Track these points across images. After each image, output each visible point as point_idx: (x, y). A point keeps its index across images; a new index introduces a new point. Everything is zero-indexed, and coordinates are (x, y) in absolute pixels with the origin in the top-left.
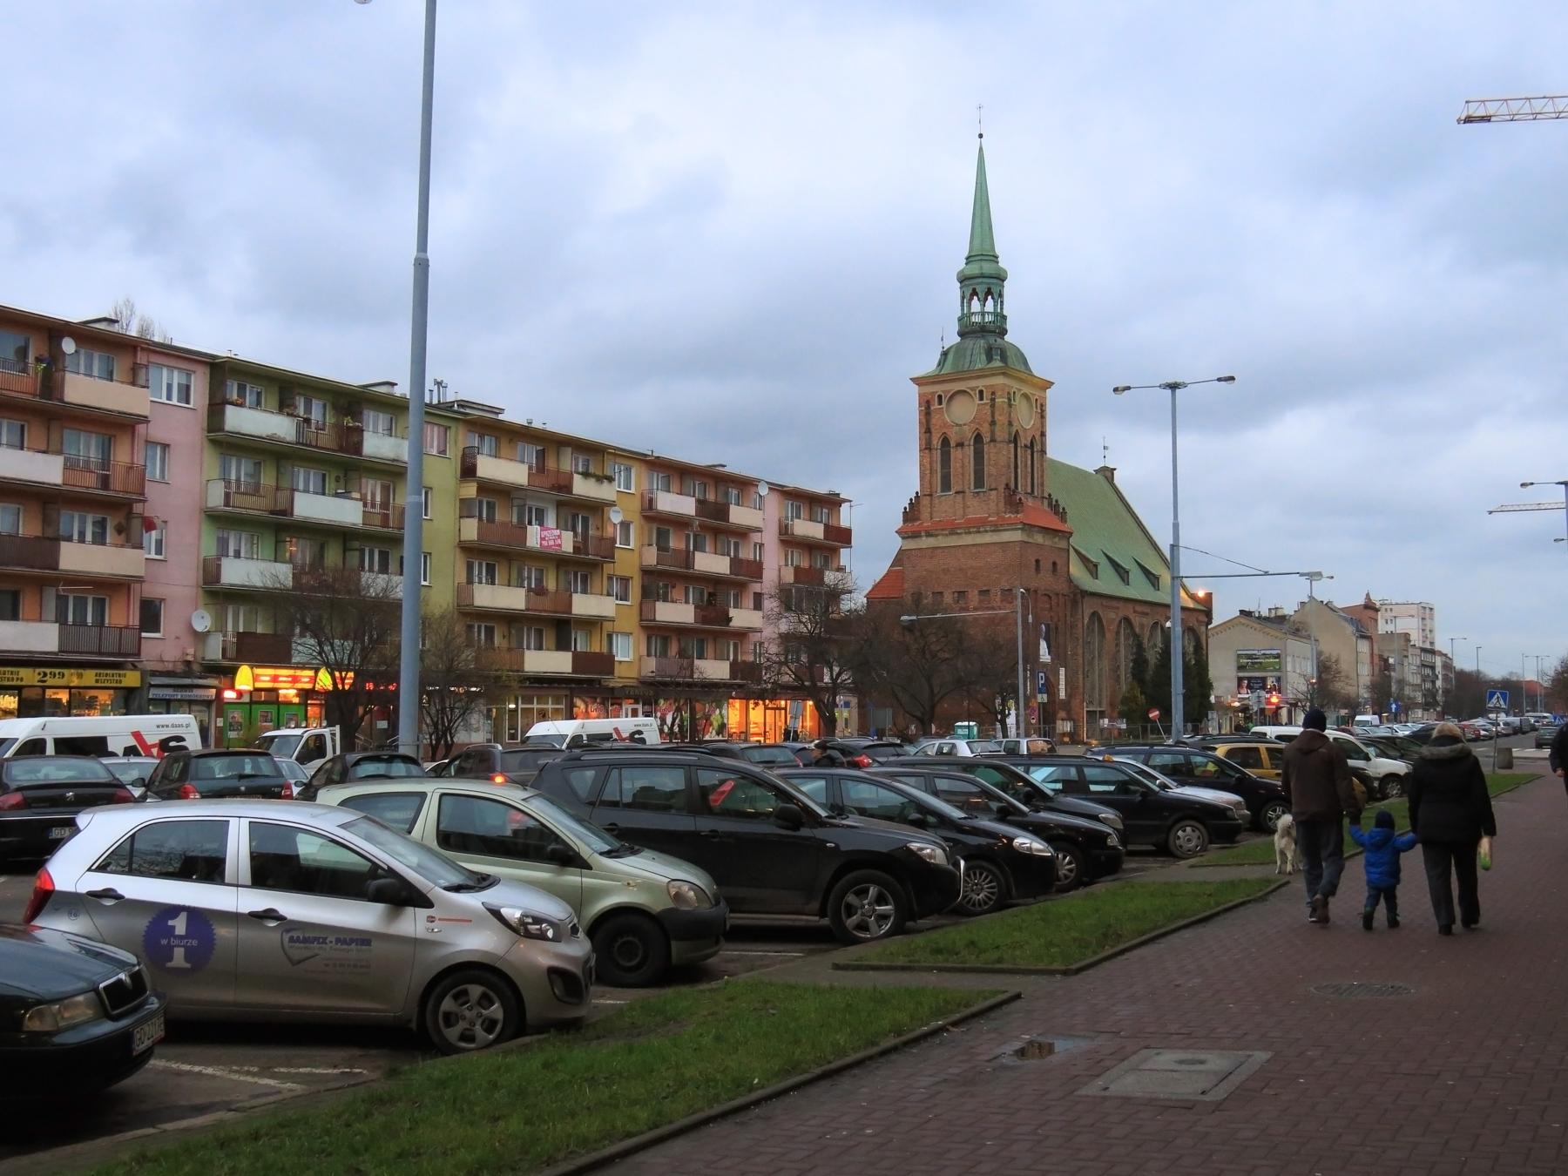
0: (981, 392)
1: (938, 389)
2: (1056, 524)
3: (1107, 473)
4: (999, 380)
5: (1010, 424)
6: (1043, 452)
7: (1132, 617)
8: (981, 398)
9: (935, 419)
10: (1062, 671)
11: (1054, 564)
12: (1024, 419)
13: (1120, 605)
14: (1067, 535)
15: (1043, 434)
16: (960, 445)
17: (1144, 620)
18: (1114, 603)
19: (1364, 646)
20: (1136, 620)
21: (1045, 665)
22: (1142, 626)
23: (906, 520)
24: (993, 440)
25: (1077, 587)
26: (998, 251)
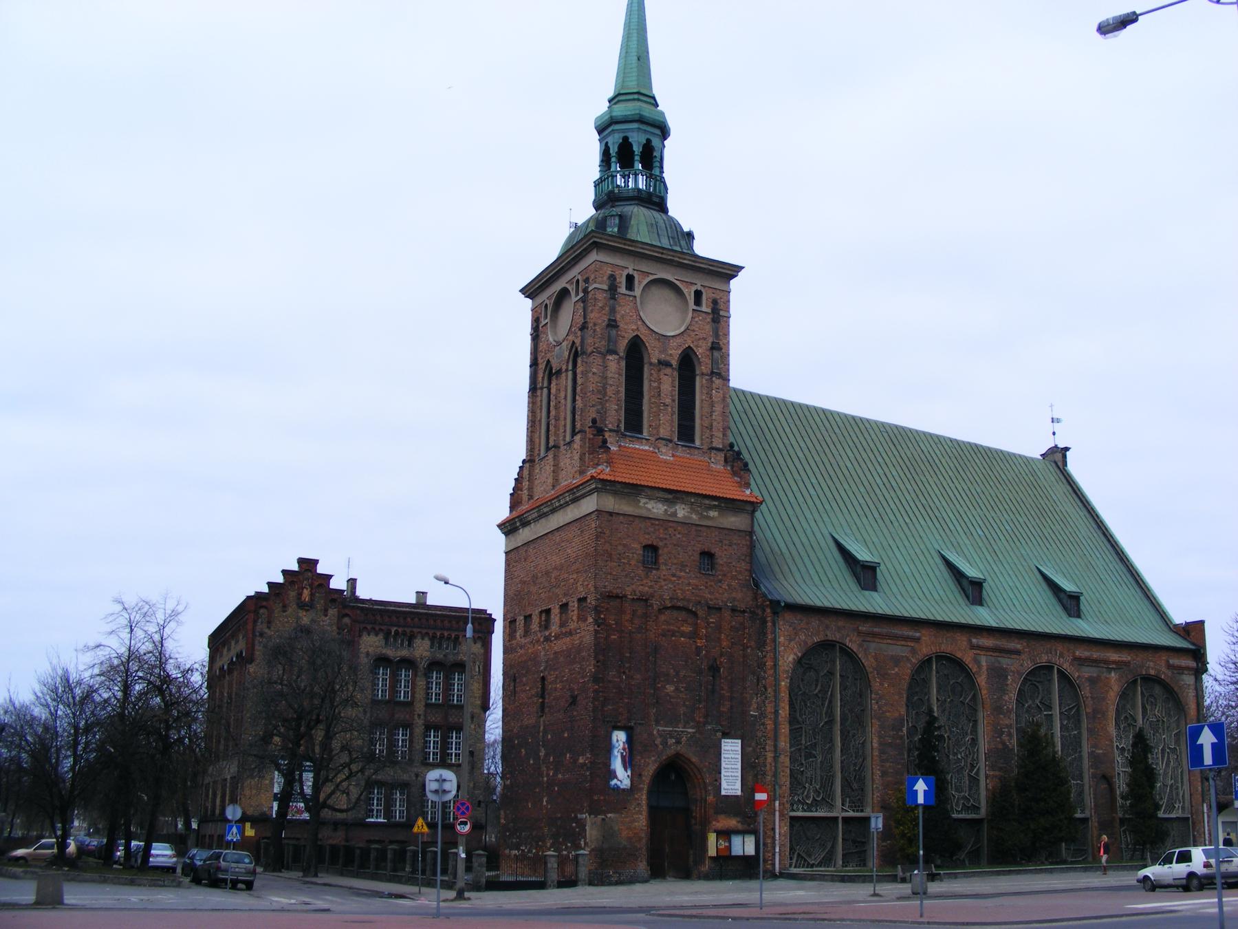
0: (578, 281)
2: (729, 490)
3: (1057, 456)
4: (594, 256)
5: (612, 324)
6: (720, 372)
7: (967, 658)
8: (577, 294)
9: (542, 346)
10: (731, 750)
11: (708, 555)
12: (663, 319)
13: (926, 635)
16: (559, 372)
17: (1005, 662)
23: (512, 508)
24: (583, 353)
25: (764, 595)
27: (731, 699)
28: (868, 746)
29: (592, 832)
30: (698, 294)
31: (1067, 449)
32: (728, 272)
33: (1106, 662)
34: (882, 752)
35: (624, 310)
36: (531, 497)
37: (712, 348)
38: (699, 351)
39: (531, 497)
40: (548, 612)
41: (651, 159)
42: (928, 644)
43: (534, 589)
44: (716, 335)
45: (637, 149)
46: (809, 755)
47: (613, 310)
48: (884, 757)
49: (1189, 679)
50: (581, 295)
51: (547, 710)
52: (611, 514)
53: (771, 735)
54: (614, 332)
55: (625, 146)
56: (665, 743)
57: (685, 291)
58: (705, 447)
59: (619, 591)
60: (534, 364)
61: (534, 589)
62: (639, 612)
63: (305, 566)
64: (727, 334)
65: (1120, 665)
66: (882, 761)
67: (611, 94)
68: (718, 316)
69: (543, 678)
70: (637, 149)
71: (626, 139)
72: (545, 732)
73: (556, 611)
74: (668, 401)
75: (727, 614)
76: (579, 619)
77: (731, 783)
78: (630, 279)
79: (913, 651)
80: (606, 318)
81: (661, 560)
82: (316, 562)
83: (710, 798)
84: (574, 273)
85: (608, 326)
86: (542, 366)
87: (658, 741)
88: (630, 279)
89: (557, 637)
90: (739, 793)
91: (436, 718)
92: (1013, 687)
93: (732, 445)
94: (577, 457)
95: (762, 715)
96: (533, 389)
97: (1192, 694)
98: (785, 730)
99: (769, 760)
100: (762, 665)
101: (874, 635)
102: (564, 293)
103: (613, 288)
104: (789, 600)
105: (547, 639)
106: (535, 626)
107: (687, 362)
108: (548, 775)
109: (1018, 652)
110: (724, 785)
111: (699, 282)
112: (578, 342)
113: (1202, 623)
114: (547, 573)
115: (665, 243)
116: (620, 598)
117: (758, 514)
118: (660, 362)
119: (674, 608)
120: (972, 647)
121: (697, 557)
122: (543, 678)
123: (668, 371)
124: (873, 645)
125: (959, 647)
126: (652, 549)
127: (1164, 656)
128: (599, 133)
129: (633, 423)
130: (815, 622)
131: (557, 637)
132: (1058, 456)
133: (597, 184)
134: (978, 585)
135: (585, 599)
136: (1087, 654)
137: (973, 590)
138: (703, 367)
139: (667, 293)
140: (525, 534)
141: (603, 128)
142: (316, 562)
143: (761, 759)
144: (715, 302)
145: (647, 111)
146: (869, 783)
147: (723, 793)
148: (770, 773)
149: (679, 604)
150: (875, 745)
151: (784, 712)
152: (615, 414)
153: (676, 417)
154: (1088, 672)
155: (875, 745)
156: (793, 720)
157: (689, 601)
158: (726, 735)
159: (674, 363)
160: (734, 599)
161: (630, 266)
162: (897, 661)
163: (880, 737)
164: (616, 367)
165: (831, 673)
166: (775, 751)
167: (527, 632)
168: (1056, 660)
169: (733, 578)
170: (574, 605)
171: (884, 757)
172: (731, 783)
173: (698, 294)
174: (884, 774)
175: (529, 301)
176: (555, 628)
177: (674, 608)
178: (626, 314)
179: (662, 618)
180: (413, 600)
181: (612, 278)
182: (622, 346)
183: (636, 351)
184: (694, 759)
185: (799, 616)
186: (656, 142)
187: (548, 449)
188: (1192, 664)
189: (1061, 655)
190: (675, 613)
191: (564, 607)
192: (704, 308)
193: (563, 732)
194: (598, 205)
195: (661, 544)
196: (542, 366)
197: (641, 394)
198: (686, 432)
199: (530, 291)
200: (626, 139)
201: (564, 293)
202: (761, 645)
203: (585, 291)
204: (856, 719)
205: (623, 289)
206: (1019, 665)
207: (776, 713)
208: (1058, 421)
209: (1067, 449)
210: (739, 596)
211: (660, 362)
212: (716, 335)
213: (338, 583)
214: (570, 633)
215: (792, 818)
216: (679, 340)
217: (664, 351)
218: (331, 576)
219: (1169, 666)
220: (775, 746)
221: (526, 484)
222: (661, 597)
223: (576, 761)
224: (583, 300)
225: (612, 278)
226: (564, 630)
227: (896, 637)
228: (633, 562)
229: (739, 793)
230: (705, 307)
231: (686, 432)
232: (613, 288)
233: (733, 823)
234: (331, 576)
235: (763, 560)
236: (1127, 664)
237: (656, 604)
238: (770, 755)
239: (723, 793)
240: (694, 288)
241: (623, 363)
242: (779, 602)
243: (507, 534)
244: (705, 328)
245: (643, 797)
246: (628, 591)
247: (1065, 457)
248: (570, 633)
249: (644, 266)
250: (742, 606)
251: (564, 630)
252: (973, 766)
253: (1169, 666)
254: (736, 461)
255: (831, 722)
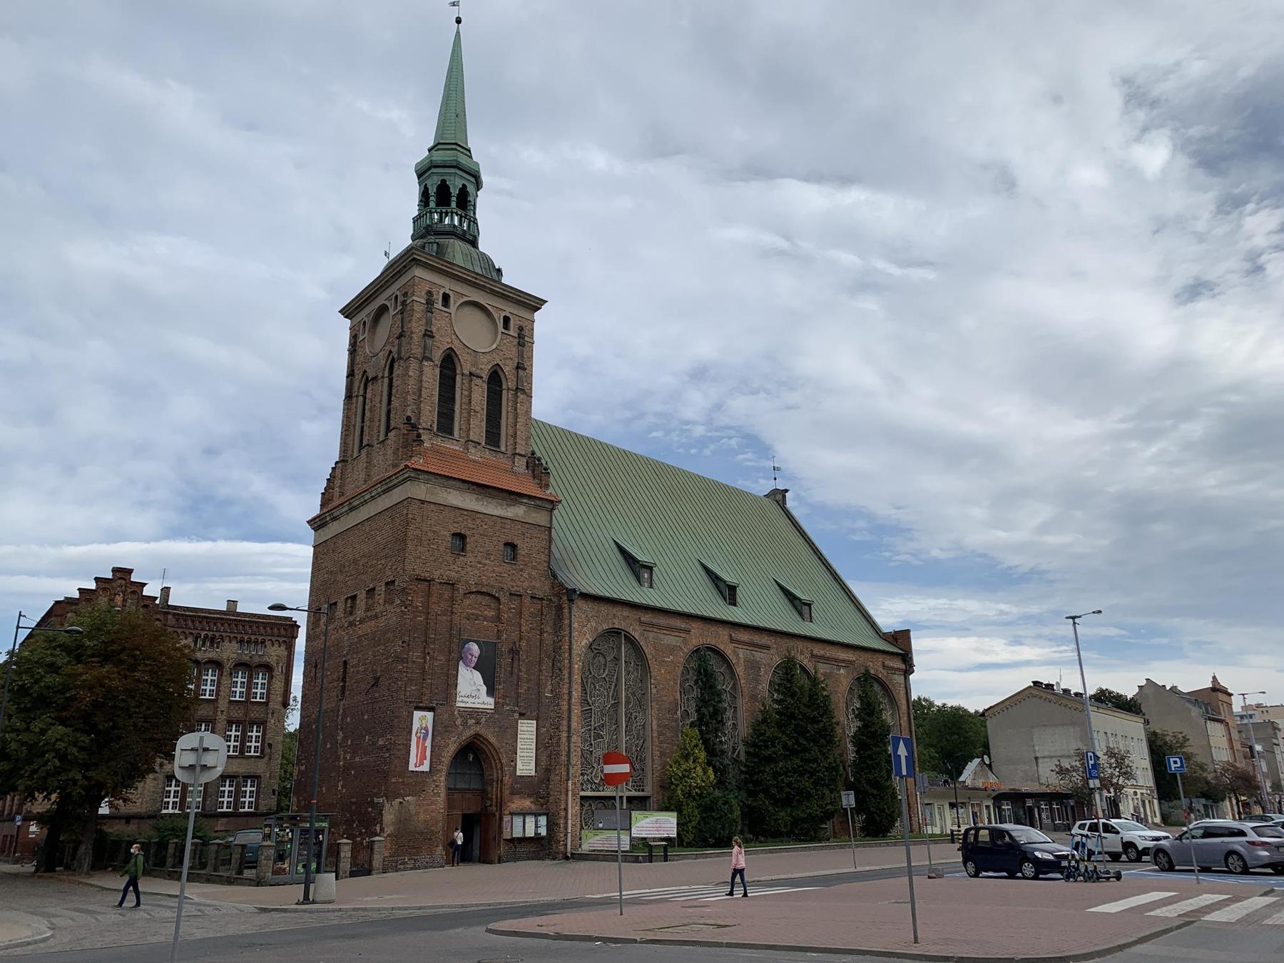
1: (362, 315)
2: (531, 488)
3: (778, 497)
5: (428, 334)
6: (523, 390)
7: (728, 650)
9: (359, 359)
10: (527, 731)
11: (511, 546)
12: (473, 336)
13: (695, 627)
14: (551, 505)
15: (523, 368)
16: (375, 379)
17: (758, 655)
18: (678, 623)
19: (1216, 732)
20: (739, 656)
21: (474, 713)
22: (753, 666)
23: (322, 506)
25: (561, 585)
26: (471, 144)
27: (528, 681)
28: (648, 727)
29: (389, 816)
30: (506, 320)
31: (786, 491)
32: (534, 304)
33: (836, 660)
34: (660, 734)
35: (438, 325)
36: (342, 494)
37: (518, 368)
38: (506, 369)
39: (342, 494)
40: (354, 598)
41: (465, 202)
42: (698, 636)
43: (340, 578)
44: (521, 355)
45: (454, 191)
46: (599, 736)
47: (429, 322)
48: (662, 738)
49: (900, 679)
50: (399, 308)
51: (347, 693)
52: (423, 502)
53: (565, 716)
54: (429, 342)
55: (443, 190)
56: (465, 724)
57: (496, 315)
58: (509, 453)
59: (427, 575)
60: (351, 375)
61: (340, 578)
62: (446, 596)
63: (118, 575)
64: (531, 358)
65: (848, 664)
66: (661, 742)
67: (431, 144)
68: (524, 340)
69: (345, 662)
70: (454, 191)
71: (444, 181)
72: (344, 715)
73: (362, 596)
74: (478, 409)
75: (527, 600)
76: (385, 602)
77: (526, 764)
78: (446, 298)
79: (685, 641)
80: (423, 329)
81: (468, 547)
82: (130, 571)
83: (506, 779)
84: (394, 289)
85: (425, 335)
86: (358, 375)
87: (458, 722)
88: (446, 298)
89: (361, 622)
90: (533, 773)
91: (238, 714)
92: (766, 676)
93: (533, 453)
94: (390, 452)
95: (557, 696)
96: (349, 397)
97: (903, 692)
98: (576, 711)
99: (564, 740)
100: (557, 649)
101: (653, 625)
102: (383, 309)
103: (430, 303)
104: (584, 591)
105: (351, 624)
106: (340, 612)
107: (495, 378)
108: (345, 758)
109: (768, 648)
110: (519, 765)
111: (509, 309)
112: (395, 350)
113: (908, 631)
114: (355, 561)
115: (478, 270)
116: (429, 581)
117: (556, 512)
118: (471, 374)
119: (478, 592)
120: (732, 640)
121: (501, 547)
122: (345, 662)
123: (478, 381)
124: (651, 635)
125: (721, 639)
126: (461, 537)
127: (881, 658)
128: (419, 176)
129: (445, 425)
130: (604, 609)
131: (361, 622)
132: (779, 497)
133: (415, 220)
134: (733, 589)
135: (393, 582)
136: (822, 652)
137: (729, 593)
138: (509, 382)
139: (479, 315)
140: (334, 528)
141: (423, 172)
142: (130, 571)
143: (554, 741)
144: (521, 329)
145: (463, 160)
146: (649, 762)
147: (518, 773)
148: (564, 753)
149: (484, 590)
150: (655, 727)
151: (576, 694)
152: (429, 415)
153: (484, 424)
154: (823, 668)
155: (655, 727)
156: (584, 701)
157: (492, 587)
158: (522, 715)
159: (485, 377)
160: (534, 588)
161: (447, 285)
162: (672, 650)
163: (658, 719)
164: (431, 375)
165: (617, 659)
166: (569, 731)
167: (331, 619)
168: (799, 658)
169: (534, 568)
170: (381, 588)
171: (662, 738)
172: (526, 764)
173: (506, 320)
174: (662, 754)
175: (347, 323)
176: (359, 613)
177: (478, 592)
178: (433, 343)
179: (467, 602)
180: (223, 607)
181: (429, 293)
182: (438, 356)
183: (449, 363)
184: (492, 740)
185: (591, 605)
186: (471, 188)
187: (361, 447)
188: (903, 667)
189: (802, 653)
190: (480, 598)
191: (371, 592)
192: (511, 333)
193: (363, 714)
194: (414, 238)
195: (468, 533)
196: (358, 375)
197: (453, 399)
198: (493, 437)
199: (348, 312)
200: (444, 181)
201: (383, 309)
202: (558, 627)
203: (403, 303)
204: (640, 702)
205: (439, 305)
206: (770, 659)
207: (570, 694)
208: (779, 469)
209: (786, 491)
210: (538, 585)
211: (471, 374)
212: (521, 355)
213: (152, 590)
214: (376, 617)
215: (582, 798)
216: (488, 357)
217: (475, 364)
218: (145, 584)
219: (884, 666)
220: (569, 726)
221: (338, 482)
222: (467, 582)
223: (374, 744)
224: (402, 312)
225: (429, 293)
226: (369, 614)
227: (671, 629)
228: (442, 549)
229: (533, 773)
230: (513, 332)
231: (493, 437)
232: (430, 303)
233: (527, 803)
234: (145, 584)
235: (557, 555)
236: (852, 663)
237: (461, 589)
238: (565, 735)
239: (518, 773)
240: (503, 314)
241: (438, 371)
242: (574, 591)
243: (315, 529)
244: (512, 351)
245: (442, 779)
246: (436, 574)
247: (784, 497)
248: (376, 617)
249: (459, 288)
250: (540, 594)
251: (369, 614)
252: (734, 750)
253: (884, 666)
254: (537, 468)
255: (616, 705)
